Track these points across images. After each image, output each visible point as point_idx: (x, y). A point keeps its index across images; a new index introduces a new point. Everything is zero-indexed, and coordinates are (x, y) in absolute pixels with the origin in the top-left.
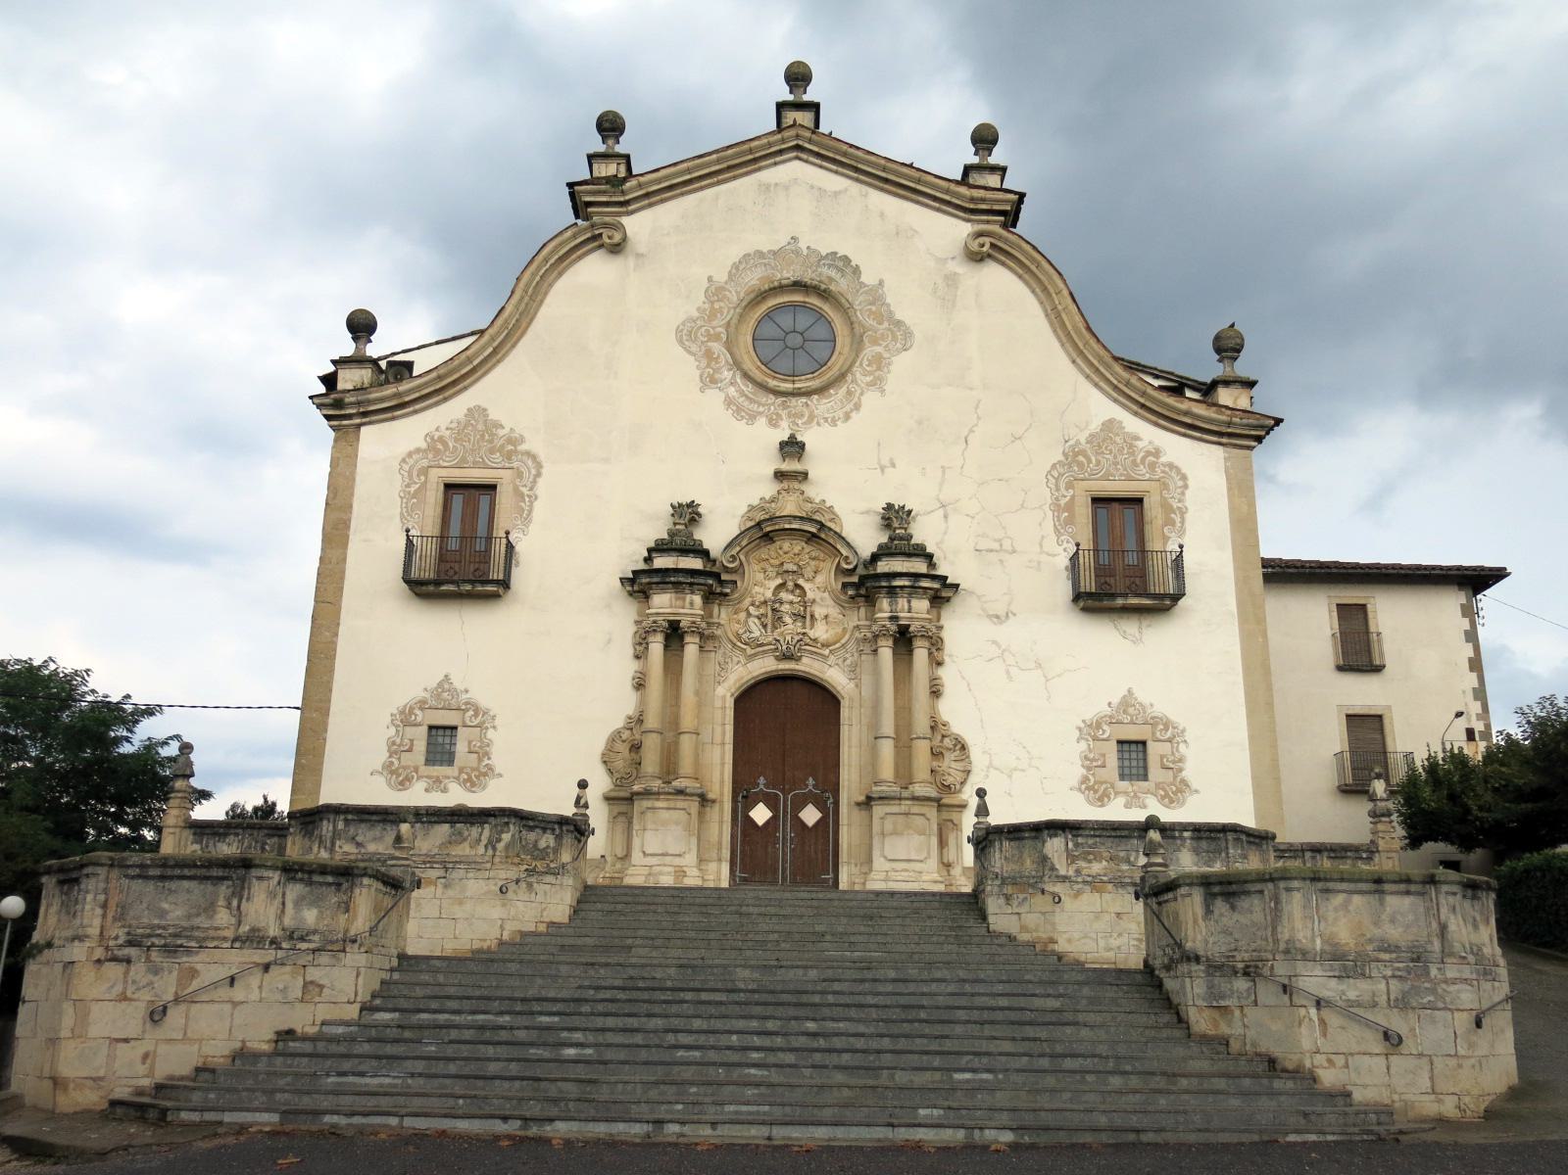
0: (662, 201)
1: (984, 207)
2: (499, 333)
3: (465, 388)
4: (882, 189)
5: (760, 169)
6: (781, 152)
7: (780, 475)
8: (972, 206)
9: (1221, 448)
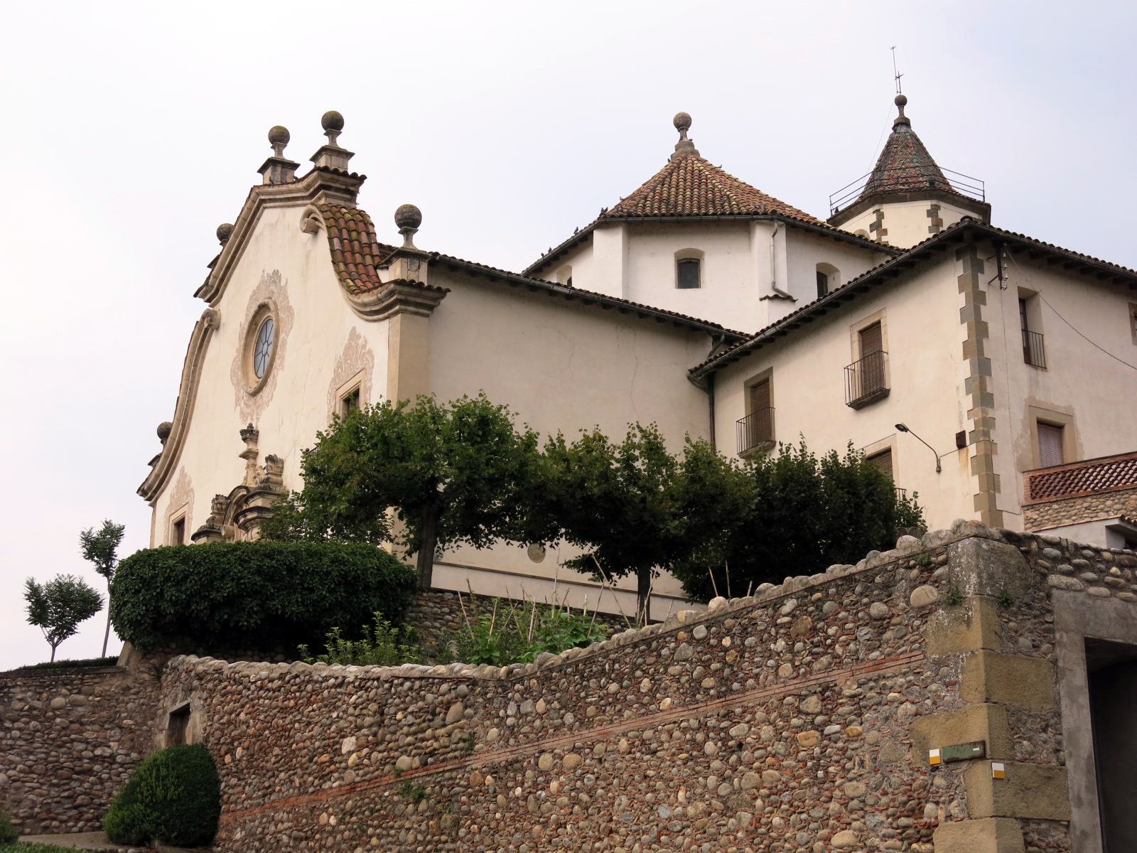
0: (229, 280)
1: (312, 190)
2: (181, 415)
3: (179, 457)
4: (289, 206)
5: (254, 228)
6: (258, 208)
7: (244, 456)
8: (308, 194)
9: (387, 321)
